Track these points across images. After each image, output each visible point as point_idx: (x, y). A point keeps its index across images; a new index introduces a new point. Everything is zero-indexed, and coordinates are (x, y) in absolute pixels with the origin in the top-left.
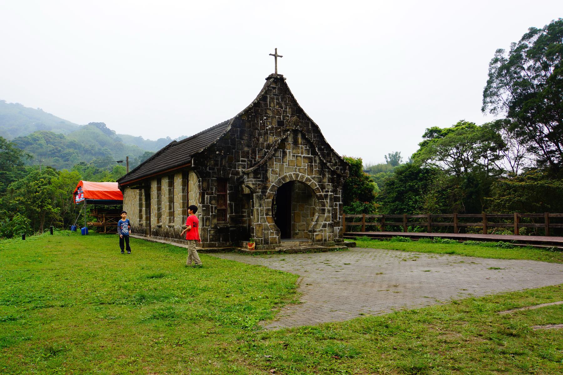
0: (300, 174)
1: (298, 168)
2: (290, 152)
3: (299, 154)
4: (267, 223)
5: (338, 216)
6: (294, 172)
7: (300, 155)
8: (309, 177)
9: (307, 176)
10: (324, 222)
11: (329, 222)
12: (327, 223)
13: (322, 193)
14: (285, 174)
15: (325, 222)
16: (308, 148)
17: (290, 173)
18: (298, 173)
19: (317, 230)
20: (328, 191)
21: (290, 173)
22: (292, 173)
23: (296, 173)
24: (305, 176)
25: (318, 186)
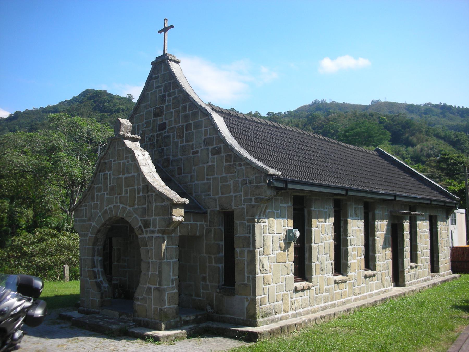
0: (121, 206)
1: (119, 196)
2: (110, 174)
3: (120, 175)
4: (88, 279)
5: (246, 275)
6: (115, 204)
7: (121, 176)
8: (131, 209)
9: (128, 208)
10: (148, 285)
11: (155, 286)
12: (153, 287)
13: (144, 235)
14: (105, 208)
15: (150, 286)
16: (130, 162)
17: (110, 206)
18: (119, 204)
19: (140, 297)
20: (153, 232)
21: (110, 206)
22: (112, 206)
23: (116, 205)
24: (127, 208)
25: (140, 224)
